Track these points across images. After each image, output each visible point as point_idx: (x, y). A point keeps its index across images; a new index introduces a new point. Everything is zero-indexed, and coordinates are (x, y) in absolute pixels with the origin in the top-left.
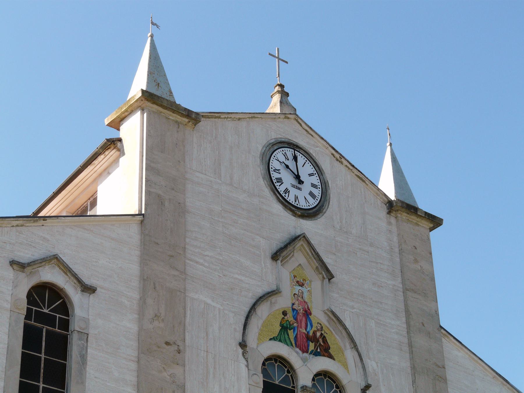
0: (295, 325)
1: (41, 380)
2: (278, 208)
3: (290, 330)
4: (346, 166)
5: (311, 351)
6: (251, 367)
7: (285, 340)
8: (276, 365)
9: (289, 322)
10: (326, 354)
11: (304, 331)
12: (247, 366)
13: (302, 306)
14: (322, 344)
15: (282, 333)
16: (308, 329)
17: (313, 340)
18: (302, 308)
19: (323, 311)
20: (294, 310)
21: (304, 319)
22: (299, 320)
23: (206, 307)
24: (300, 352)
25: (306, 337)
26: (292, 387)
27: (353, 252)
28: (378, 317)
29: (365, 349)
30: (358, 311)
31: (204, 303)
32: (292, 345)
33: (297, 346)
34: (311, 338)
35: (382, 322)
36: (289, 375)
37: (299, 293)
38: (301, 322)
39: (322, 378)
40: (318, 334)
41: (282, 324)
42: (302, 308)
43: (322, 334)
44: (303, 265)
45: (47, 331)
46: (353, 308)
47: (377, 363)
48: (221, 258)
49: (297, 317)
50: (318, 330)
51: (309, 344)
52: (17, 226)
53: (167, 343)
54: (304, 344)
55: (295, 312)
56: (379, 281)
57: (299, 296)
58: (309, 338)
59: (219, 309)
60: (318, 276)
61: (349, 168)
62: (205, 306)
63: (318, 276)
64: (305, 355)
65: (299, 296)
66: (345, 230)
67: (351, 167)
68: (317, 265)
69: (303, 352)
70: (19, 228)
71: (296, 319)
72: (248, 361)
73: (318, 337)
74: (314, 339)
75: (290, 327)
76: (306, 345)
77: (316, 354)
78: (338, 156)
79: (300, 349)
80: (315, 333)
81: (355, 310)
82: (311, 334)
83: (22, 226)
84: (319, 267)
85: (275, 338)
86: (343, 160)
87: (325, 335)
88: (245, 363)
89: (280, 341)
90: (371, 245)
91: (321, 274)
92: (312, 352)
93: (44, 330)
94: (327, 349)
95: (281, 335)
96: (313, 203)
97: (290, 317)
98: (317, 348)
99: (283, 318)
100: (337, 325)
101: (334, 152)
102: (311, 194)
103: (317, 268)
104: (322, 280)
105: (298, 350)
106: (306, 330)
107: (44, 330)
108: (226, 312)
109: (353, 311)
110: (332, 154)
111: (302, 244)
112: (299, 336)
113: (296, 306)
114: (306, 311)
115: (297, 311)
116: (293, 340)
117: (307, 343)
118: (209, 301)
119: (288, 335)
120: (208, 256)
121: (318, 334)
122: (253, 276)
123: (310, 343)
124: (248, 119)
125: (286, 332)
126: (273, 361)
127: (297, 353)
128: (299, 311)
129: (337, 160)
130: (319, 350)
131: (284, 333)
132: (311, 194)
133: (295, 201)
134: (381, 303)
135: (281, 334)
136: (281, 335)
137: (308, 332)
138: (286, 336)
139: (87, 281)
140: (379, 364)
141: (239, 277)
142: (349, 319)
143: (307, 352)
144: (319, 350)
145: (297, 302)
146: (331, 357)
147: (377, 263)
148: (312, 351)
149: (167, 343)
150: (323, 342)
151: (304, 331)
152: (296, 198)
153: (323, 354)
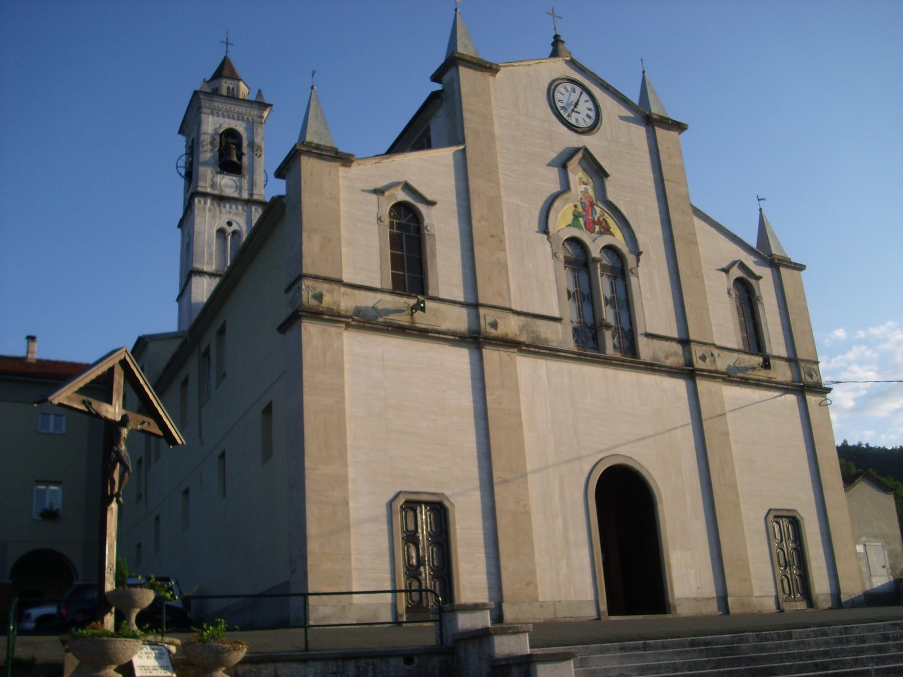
0: (584, 214)
1: (406, 270)
2: (564, 129)
6: (554, 247)
10: (609, 233)
11: (591, 218)
12: (551, 247)
14: (605, 225)
16: (594, 215)
20: (582, 203)
24: (589, 233)
32: (583, 229)
38: (588, 211)
40: (601, 219)
45: (406, 235)
52: (376, 163)
53: (492, 236)
58: (594, 223)
67: (616, 92)
70: (377, 165)
71: (584, 209)
74: (599, 223)
77: (600, 233)
80: (598, 218)
82: (596, 219)
83: (379, 162)
86: (609, 87)
88: (550, 245)
89: (574, 226)
93: (404, 235)
96: (590, 122)
97: (580, 209)
99: (575, 210)
102: (588, 116)
106: (592, 216)
107: (404, 235)
114: (591, 203)
115: (584, 203)
118: (519, 202)
119: (579, 221)
121: (601, 219)
123: (596, 226)
129: (605, 88)
132: (588, 116)
137: (594, 218)
139: (429, 197)
148: (598, 232)
149: (492, 236)
151: (591, 218)
152: (577, 120)
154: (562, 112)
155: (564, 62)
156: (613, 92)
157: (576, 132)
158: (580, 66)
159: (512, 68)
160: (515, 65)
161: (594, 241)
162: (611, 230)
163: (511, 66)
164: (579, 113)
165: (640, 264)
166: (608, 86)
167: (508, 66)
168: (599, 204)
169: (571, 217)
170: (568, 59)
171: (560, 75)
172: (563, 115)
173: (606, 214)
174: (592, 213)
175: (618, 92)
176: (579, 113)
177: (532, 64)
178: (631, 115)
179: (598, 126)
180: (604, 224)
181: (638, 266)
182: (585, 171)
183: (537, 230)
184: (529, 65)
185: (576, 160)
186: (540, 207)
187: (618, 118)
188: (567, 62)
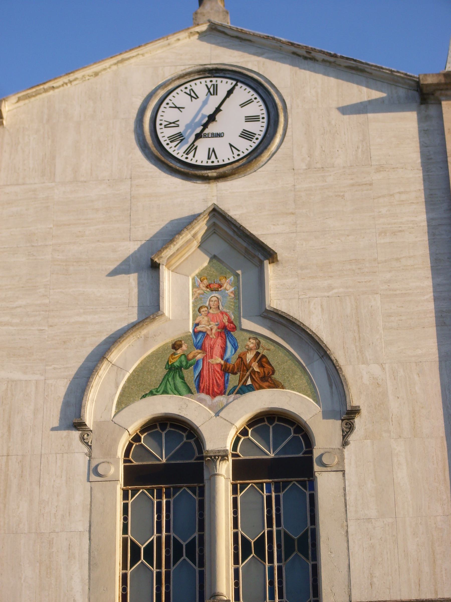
3: (187, 368)
4: (324, 61)
5: (230, 389)
7: (176, 388)
8: (164, 434)
9: (186, 357)
11: (219, 360)
13: (217, 322)
14: (257, 369)
15: (170, 379)
16: (228, 354)
17: (238, 369)
18: (217, 325)
19: (260, 316)
21: (219, 341)
22: (207, 346)
23: (10, 386)
24: (207, 398)
25: (221, 370)
26: (198, 459)
27: (336, 196)
28: (389, 286)
29: (354, 349)
30: (341, 290)
31: (6, 382)
33: (199, 389)
34: (234, 368)
35: (398, 292)
36: (192, 441)
37: (211, 303)
38: (212, 348)
39: (266, 424)
41: (170, 364)
42: (217, 325)
43: (258, 354)
44: (218, 256)
46: (330, 288)
47: (382, 365)
48: (47, 301)
49: (204, 343)
50: (250, 350)
51: (228, 379)
54: (217, 382)
55: (200, 336)
56: (395, 223)
57: (211, 308)
59: (37, 382)
60: (252, 261)
61: (330, 62)
62: (7, 386)
63: (252, 261)
64: (219, 398)
65: (211, 308)
66: (319, 166)
67: (332, 59)
68: (245, 244)
69: (214, 395)
72: (90, 446)
73: (248, 362)
75: (187, 363)
76: (221, 382)
78: (303, 52)
79: (208, 393)
81: (335, 291)
82: (233, 361)
84: (250, 248)
85: (154, 391)
86: (313, 54)
87: (265, 353)
89: (165, 392)
90: (380, 169)
91: (254, 256)
92: (234, 391)
94: (268, 374)
95: (168, 382)
98: (246, 381)
99: (174, 354)
100: (290, 328)
101: (293, 49)
103: (246, 250)
104: (260, 266)
105: (203, 396)
106: (222, 358)
108: (50, 382)
109: (330, 294)
110: (294, 53)
111: (214, 222)
112: (205, 373)
113: (204, 326)
115: (204, 333)
116: (193, 382)
117: (225, 378)
118: (17, 375)
119: (182, 378)
120: (20, 307)
121: (250, 356)
122: (111, 308)
123: (231, 377)
124: (114, 68)
125: (177, 375)
126: (159, 429)
127: (201, 400)
128: (209, 333)
129: (305, 58)
130: (249, 382)
131: (173, 378)
133: (209, 158)
134: (398, 259)
135: (168, 380)
136: (166, 383)
137: (227, 361)
138: (178, 381)
140: (387, 366)
141: (81, 319)
142: (320, 309)
143: (222, 393)
144: (249, 382)
145: (206, 318)
146: (275, 385)
147: (392, 195)
148: (235, 388)
150: (261, 365)
151: (219, 360)
153: (259, 385)
154: (172, 148)
155: (196, 36)
156: (324, 61)
157: (206, 179)
158: (235, 34)
159: (51, 93)
160: (55, 85)
161: (217, 414)
162: (277, 376)
163: (46, 91)
164: (219, 135)
165: (352, 438)
166: (309, 51)
167: (37, 94)
168: (247, 324)
169: (162, 371)
170: (204, 28)
171: (183, 68)
172: (174, 154)
173: (263, 342)
174: (224, 350)
175: (335, 56)
176: (219, 135)
177: (105, 69)
178: (376, 94)
179: (273, 147)
180: (255, 367)
181: (345, 443)
182: (219, 260)
183: (56, 423)
184: (96, 74)
185: (188, 242)
186: (73, 372)
187: (336, 114)
188: (202, 36)
